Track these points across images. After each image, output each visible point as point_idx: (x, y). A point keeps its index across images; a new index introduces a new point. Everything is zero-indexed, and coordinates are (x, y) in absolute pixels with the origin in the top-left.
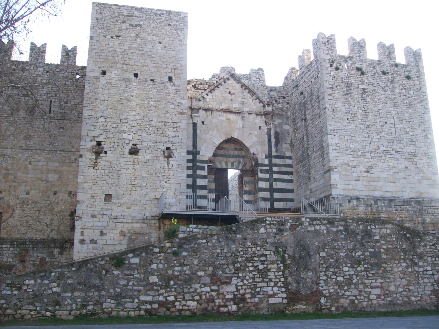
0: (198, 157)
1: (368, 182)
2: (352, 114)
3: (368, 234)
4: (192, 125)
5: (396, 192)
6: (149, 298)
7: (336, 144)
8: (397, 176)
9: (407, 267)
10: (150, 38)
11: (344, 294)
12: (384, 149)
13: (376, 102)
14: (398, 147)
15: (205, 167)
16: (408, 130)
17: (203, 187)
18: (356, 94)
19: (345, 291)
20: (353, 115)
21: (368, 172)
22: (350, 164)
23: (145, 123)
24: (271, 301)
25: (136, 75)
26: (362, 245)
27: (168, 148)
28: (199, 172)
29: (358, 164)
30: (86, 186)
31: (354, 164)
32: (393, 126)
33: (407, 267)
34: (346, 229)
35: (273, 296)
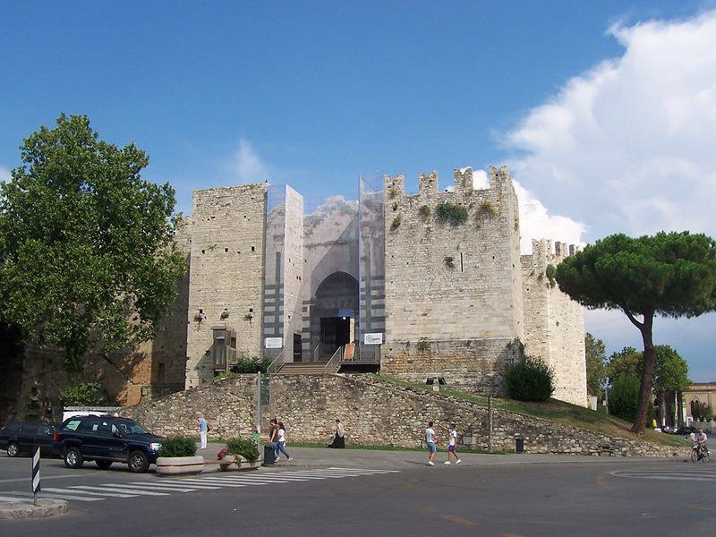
1: (425, 325)
3: (316, 385)
5: (456, 333)
6: (168, 428)
7: (393, 292)
8: (459, 316)
10: (237, 214)
13: (441, 240)
18: (420, 235)
21: (426, 315)
24: (241, 432)
25: (227, 250)
26: (311, 394)
27: (251, 310)
34: (298, 382)
35: (243, 429)
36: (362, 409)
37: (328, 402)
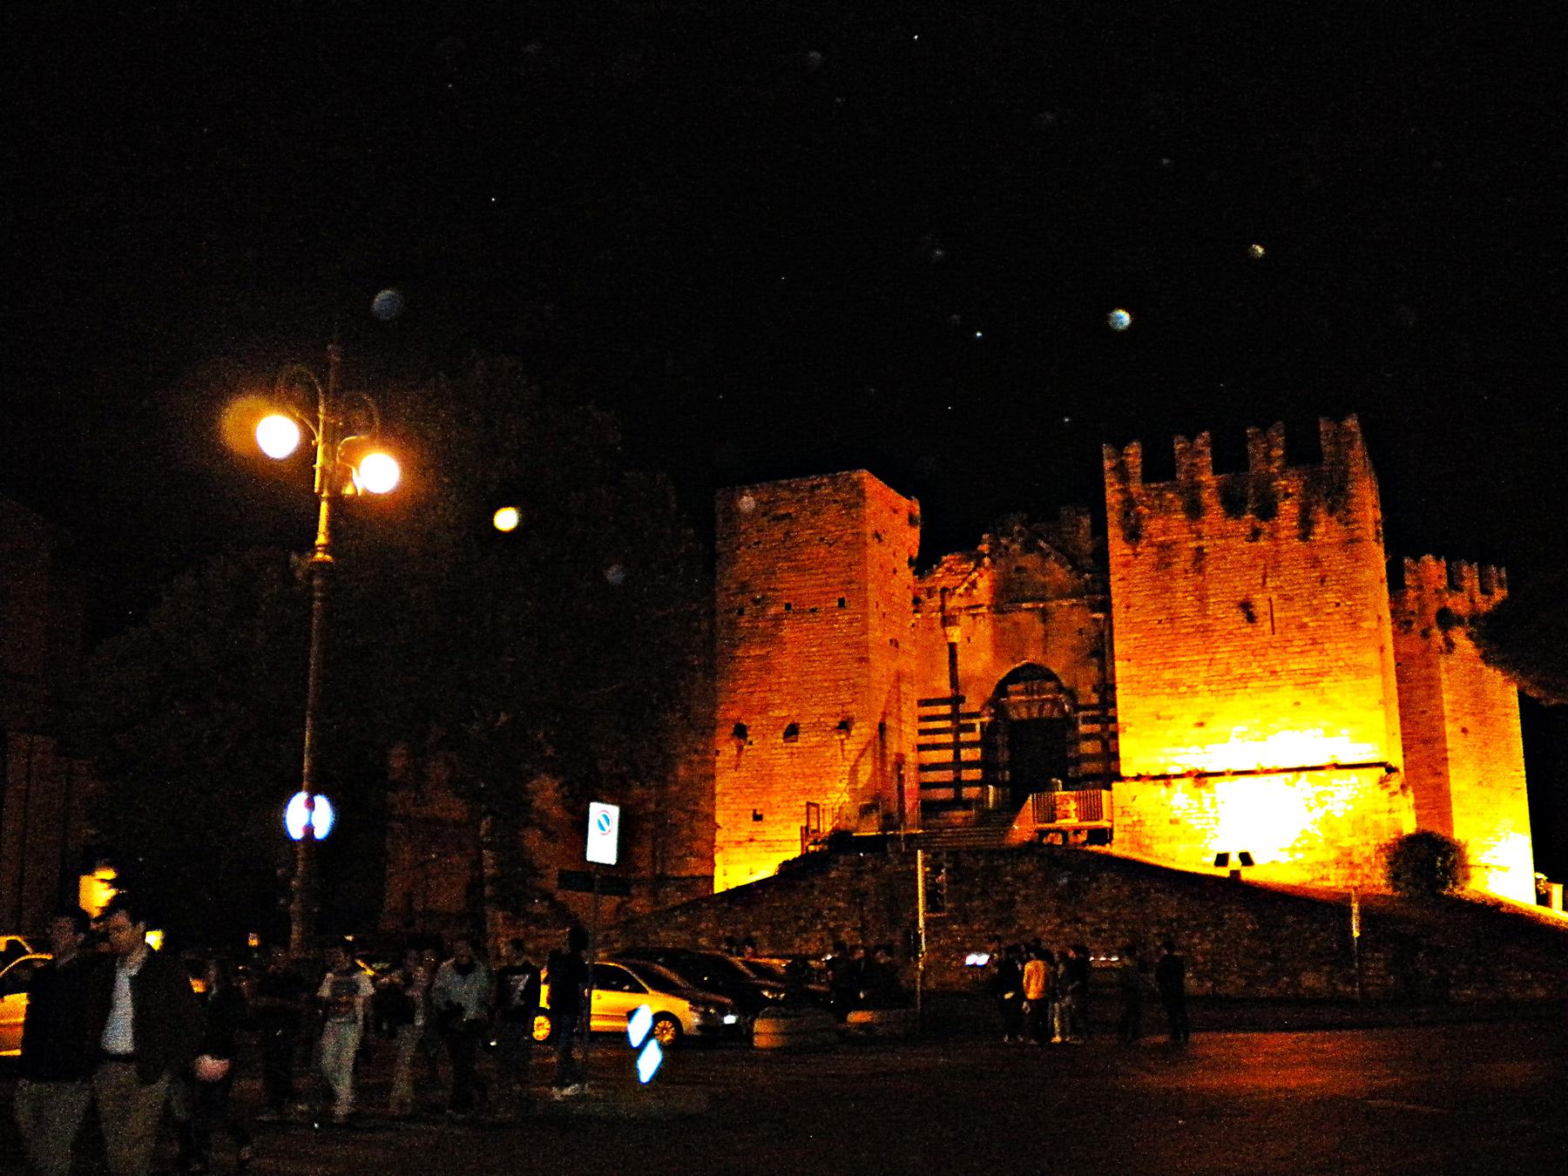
0: (962, 709)
2: (1169, 608)
4: (947, 648)
9: (1061, 925)
11: (949, 964)
12: (1242, 671)
14: (1278, 662)
15: (974, 725)
16: (1306, 620)
17: (971, 765)
19: (953, 959)
20: (1172, 611)
21: (1201, 724)
22: (1162, 713)
23: (806, 686)
28: (963, 737)
29: (1180, 712)
30: (727, 799)
31: (1170, 713)
32: (1268, 617)
33: (1061, 925)
36: (1088, 919)
37: (1018, 906)
